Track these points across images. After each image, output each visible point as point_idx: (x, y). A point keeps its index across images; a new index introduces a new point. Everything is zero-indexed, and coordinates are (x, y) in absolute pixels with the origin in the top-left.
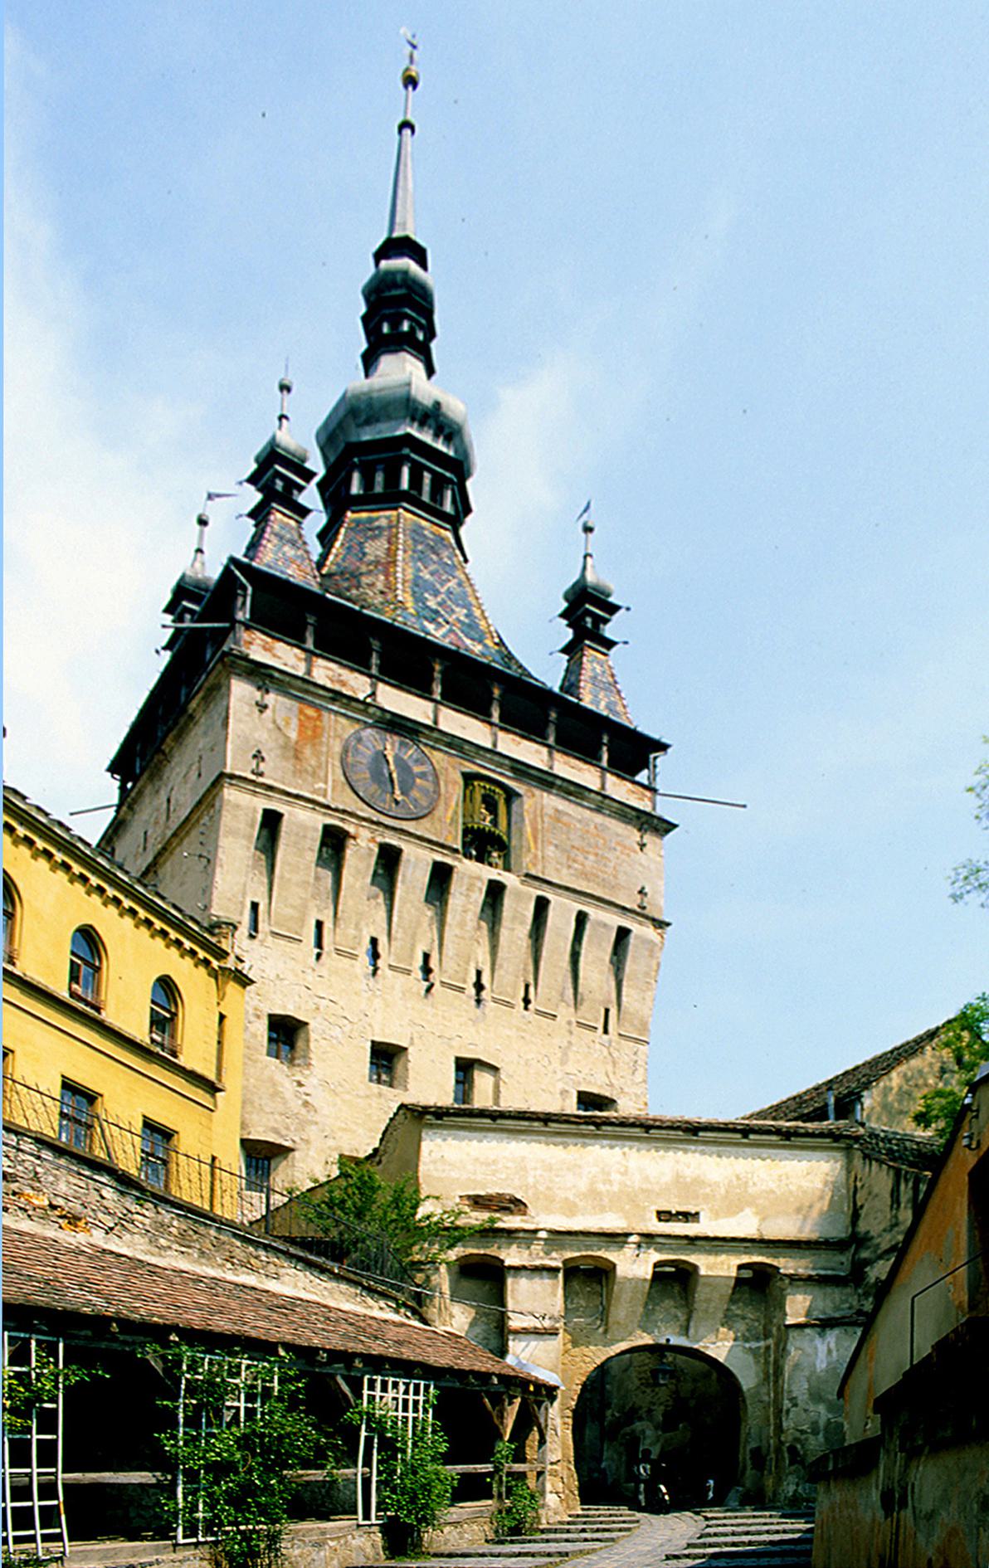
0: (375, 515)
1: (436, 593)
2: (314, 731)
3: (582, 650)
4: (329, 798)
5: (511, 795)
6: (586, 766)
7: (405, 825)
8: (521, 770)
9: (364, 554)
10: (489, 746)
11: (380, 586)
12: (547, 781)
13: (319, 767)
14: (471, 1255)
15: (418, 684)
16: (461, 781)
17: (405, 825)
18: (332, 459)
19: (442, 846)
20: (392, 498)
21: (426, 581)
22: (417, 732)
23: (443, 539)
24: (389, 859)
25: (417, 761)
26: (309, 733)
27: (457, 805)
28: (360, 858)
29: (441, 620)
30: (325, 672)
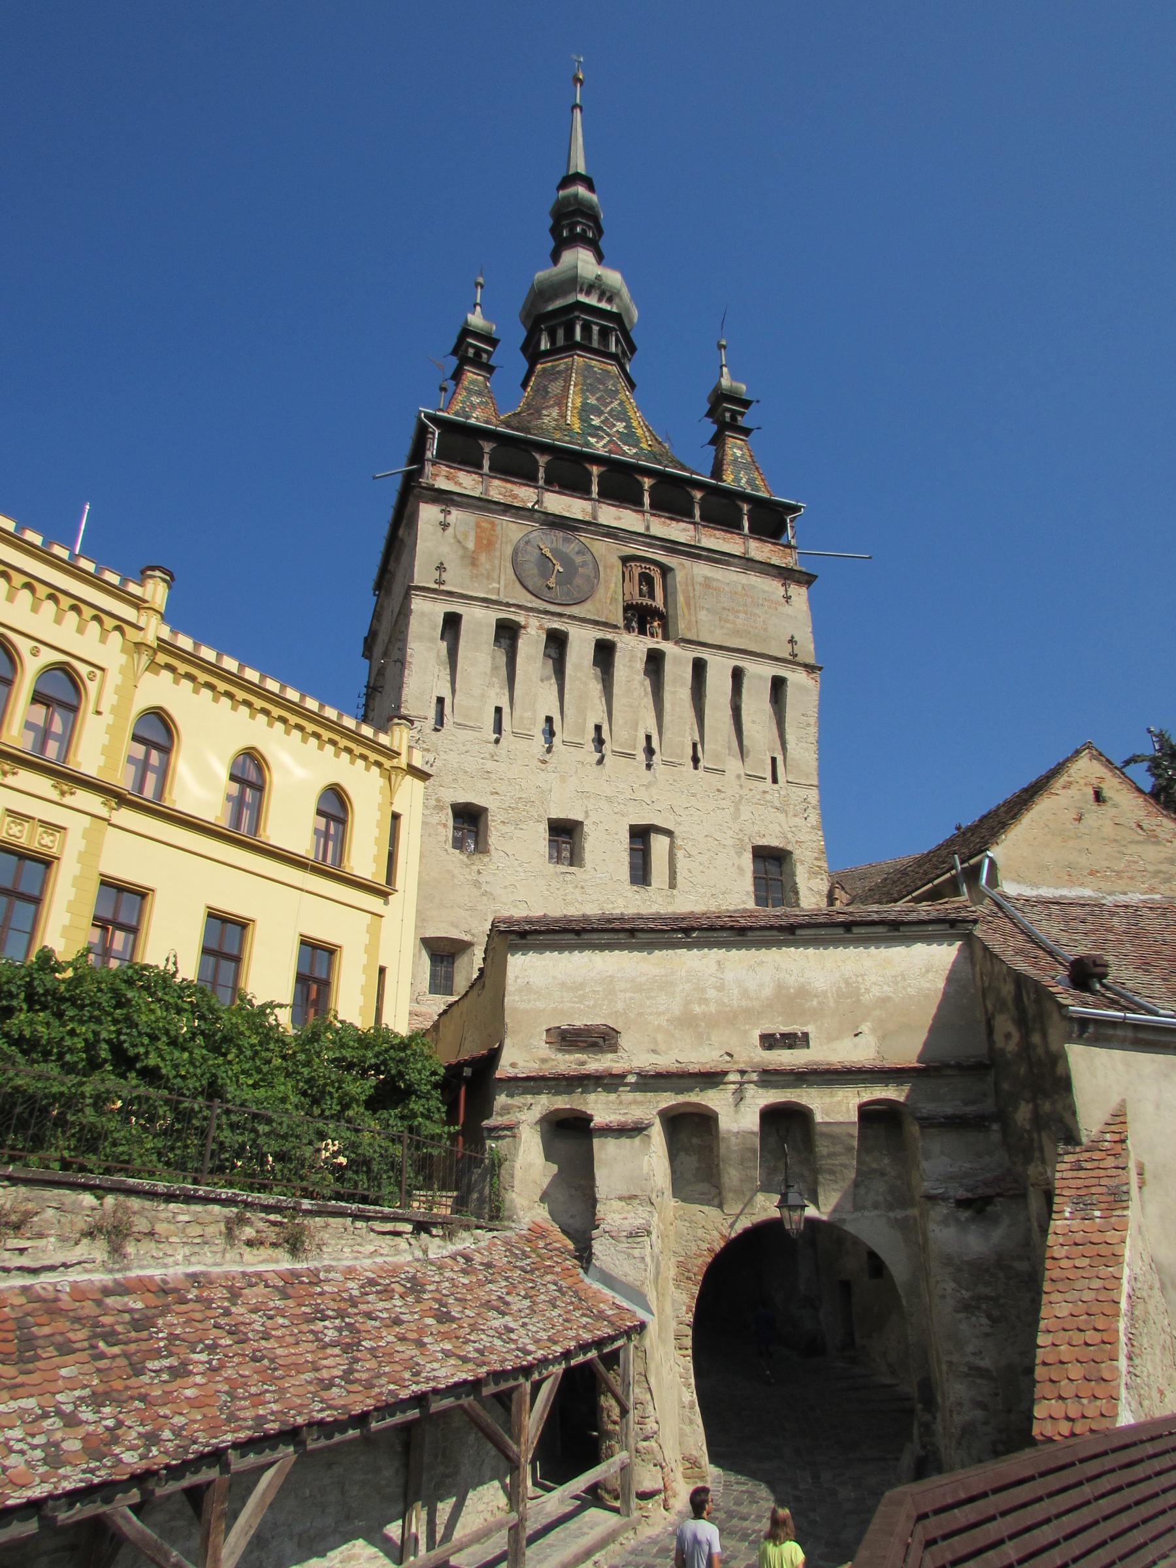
0: (556, 363)
1: (599, 413)
2: (488, 540)
3: (724, 440)
4: (502, 596)
5: (665, 570)
6: (729, 536)
7: (568, 611)
8: (672, 547)
9: (547, 393)
10: (642, 530)
11: (555, 412)
12: (693, 552)
13: (493, 569)
14: (557, 1110)
15: (579, 488)
16: (620, 563)
17: (568, 611)
18: (529, 327)
19: (606, 624)
20: (571, 347)
21: (593, 405)
22: (577, 529)
23: (609, 372)
24: (557, 642)
25: (578, 553)
26: (485, 542)
27: (616, 586)
28: (531, 644)
29: (601, 434)
30: (498, 490)
